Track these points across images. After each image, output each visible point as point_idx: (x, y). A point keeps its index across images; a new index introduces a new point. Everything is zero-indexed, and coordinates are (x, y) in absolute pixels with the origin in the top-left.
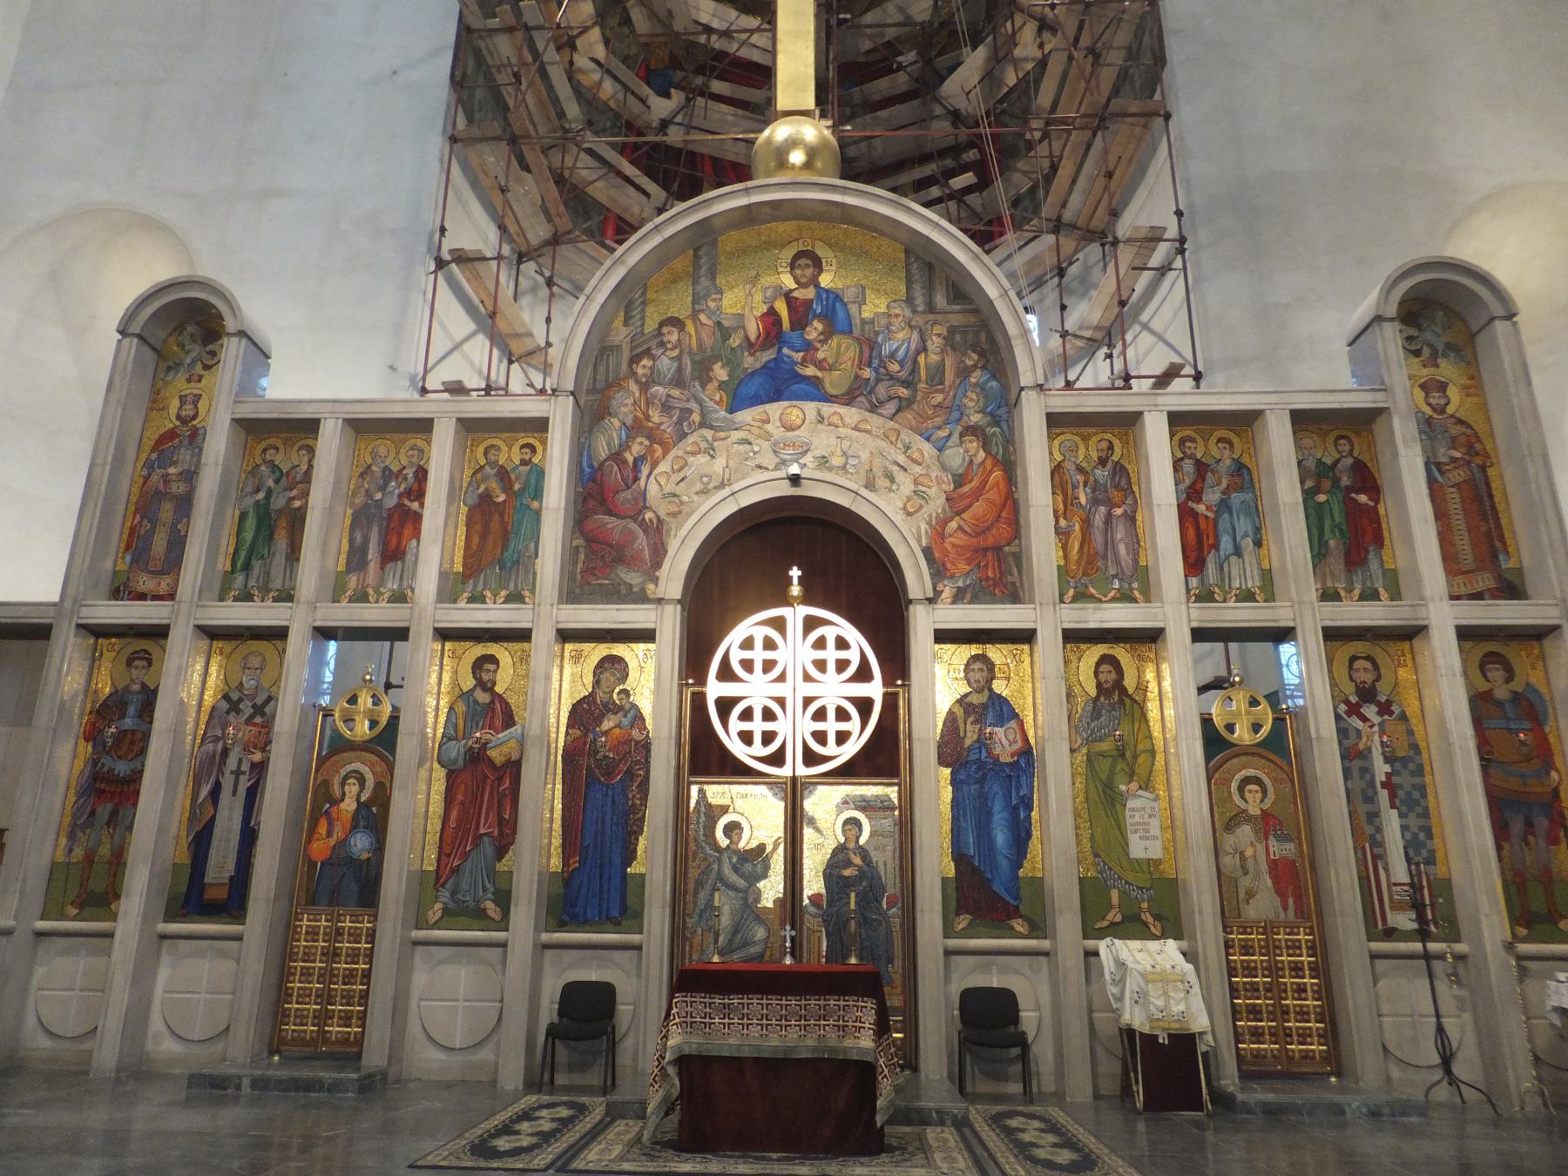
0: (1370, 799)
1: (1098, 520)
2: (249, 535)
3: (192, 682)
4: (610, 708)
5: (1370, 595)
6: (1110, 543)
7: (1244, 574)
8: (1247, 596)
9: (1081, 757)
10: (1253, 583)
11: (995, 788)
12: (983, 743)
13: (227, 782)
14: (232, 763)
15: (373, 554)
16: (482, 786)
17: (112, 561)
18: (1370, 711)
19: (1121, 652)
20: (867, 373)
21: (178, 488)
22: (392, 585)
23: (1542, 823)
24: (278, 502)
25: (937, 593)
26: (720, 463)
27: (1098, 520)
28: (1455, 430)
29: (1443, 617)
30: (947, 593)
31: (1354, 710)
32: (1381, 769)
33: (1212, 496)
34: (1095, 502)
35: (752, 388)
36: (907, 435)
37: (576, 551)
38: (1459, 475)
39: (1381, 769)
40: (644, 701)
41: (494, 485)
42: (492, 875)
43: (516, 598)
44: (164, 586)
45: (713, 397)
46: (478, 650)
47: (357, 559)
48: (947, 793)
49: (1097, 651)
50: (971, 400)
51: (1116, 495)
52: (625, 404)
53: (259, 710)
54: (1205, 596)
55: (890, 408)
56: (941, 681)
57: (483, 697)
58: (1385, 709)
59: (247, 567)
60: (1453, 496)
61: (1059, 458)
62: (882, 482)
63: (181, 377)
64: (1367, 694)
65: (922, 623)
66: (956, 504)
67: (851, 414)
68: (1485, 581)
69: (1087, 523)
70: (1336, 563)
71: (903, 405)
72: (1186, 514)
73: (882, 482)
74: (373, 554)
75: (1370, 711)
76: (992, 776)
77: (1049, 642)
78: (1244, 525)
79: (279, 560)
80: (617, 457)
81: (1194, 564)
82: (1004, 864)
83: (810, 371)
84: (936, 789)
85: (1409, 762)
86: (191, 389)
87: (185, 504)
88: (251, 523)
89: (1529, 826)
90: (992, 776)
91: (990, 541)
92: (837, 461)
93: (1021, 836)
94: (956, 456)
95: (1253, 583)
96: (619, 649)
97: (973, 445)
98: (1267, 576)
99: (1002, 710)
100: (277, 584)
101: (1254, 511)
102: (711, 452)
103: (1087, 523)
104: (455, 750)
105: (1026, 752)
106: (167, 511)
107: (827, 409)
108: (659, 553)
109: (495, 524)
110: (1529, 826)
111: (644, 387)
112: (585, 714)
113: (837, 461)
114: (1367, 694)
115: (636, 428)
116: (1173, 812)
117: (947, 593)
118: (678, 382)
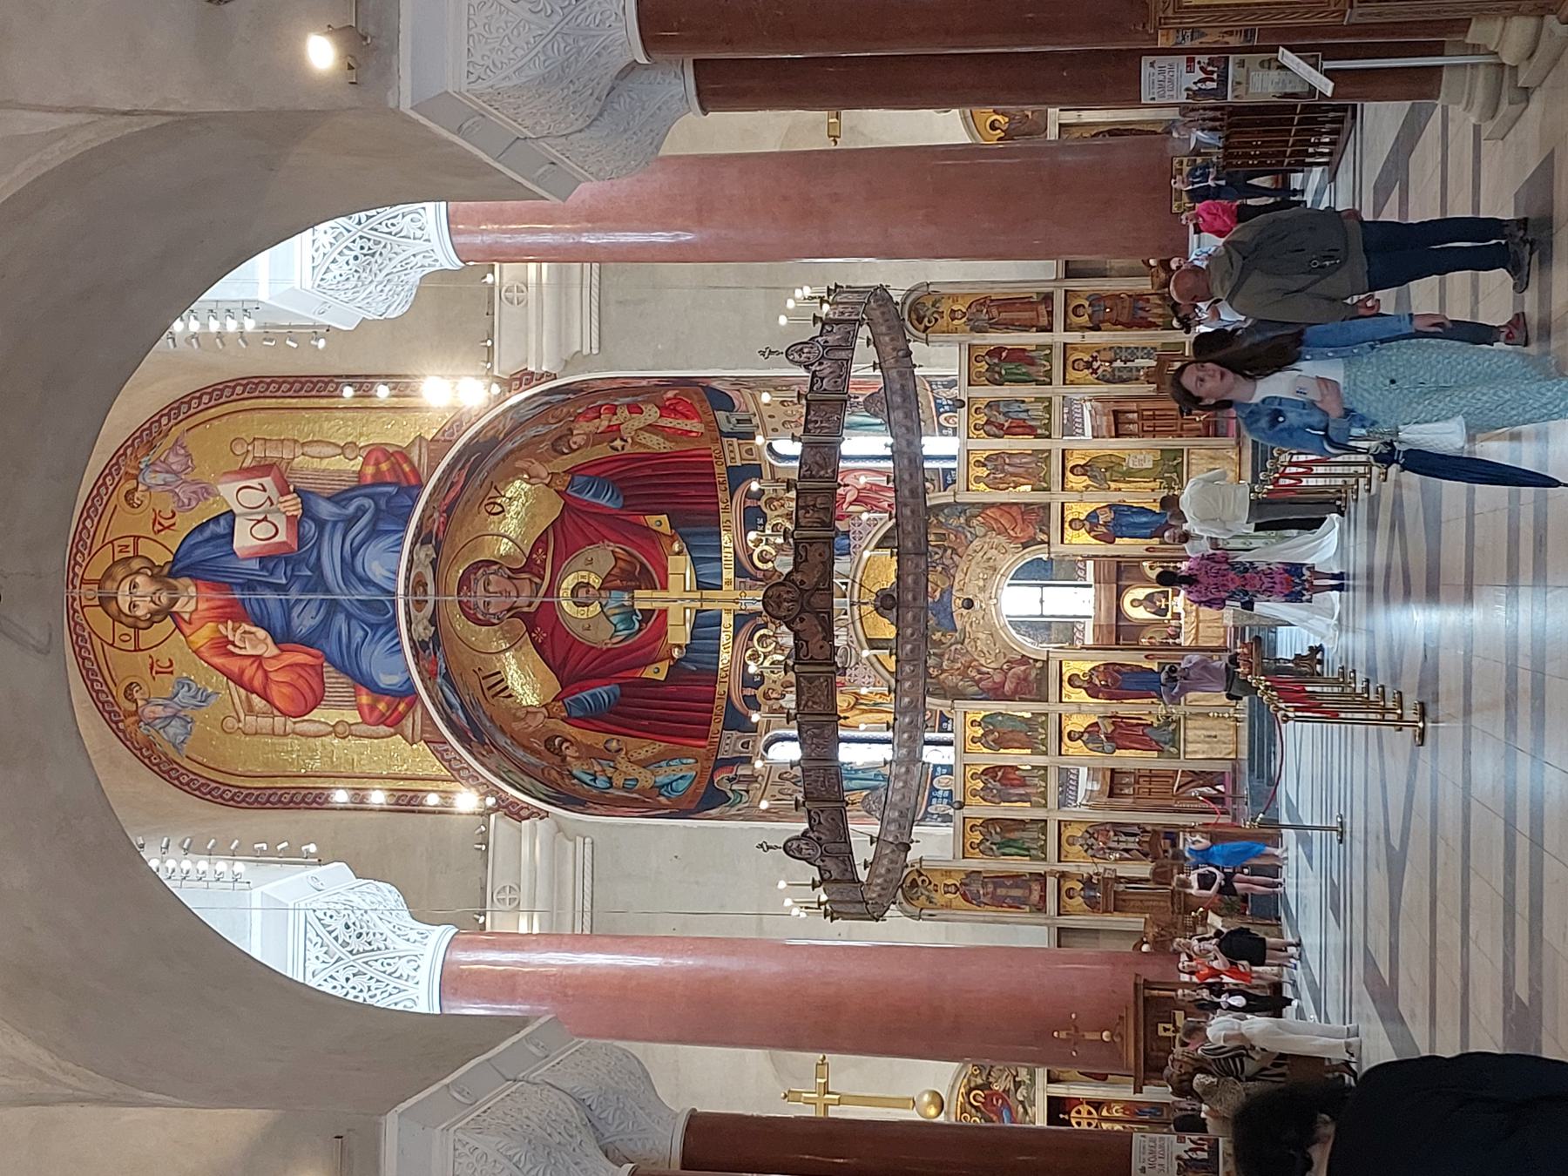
0: (1131, 369)
1: (1011, 469)
2: (1013, 850)
3: (1082, 865)
4: (1090, 681)
5: (1048, 358)
6: (1021, 465)
7: (1037, 410)
8: (1048, 409)
9: (1113, 485)
10: (1041, 406)
11: (1125, 520)
12: (1106, 524)
13: (1123, 846)
14: (1114, 845)
15: (1022, 791)
16: (1122, 733)
17: (1024, 915)
18: (1096, 365)
19: (1069, 465)
20: (939, 568)
21: (990, 888)
22: (1036, 781)
23: (1141, 304)
24: (998, 839)
25: (1043, 542)
26: (980, 635)
27: (1011, 469)
28: (974, 309)
29: (1059, 336)
30: (1044, 537)
31: (1095, 371)
32: (1118, 364)
33: (1001, 419)
34: (1003, 471)
35: (946, 622)
36: (970, 551)
37: (1021, 700)
38: (995, 312)
39: (1118, 364)
40: (1088, 666)
41: (990, 738)
42: (1159, 727)
43: (1044, 725)
44: (1036, 887)
45: (948, 640)
46: (1065, 739)
47: (1023, 798)
48: (1126, 540)
49: (1068, 474)
50: (954, 522)
51: (1000, 461)
52: (951, 680)
53: (1092, 835)
54: (1048, 426)
55: (956, 558)
56: (1081, 540)
57: (1086, 736)
58: (1095, 359)
59: (1028, 849)
60: (1003, 315)
61: (982, 486)
62: (991, 563)
63: (933, 895)
64: (1089, 365)
65: (1057, 548)
66: (1003, 531)
67: (959, 576)
68: (1042, 309)
69: (1012, 475)
70: (1032, 369)
71: (954, 551)
72: (1010, 432)
73: (991, 563)
74: (1022, 791)
75: (1096, 365)
76: (1121, 521)
77: (1063, 497)
78: (1015, 407)
79: (1025, 834)
80: (977, 683)
81: (1031, 431)
82: (1155, 518)
83: (938, 594)
84: (1127, 546)
85: (1117, 352)
86: (941, 889)
87: (999, 879)
88: (1007, 850)
89: (1142, 309)
90: (1121, 521)
91: (1019, 517)
92: (981, 583)
93: (1143, 511)
94: (980, 531)
95: (1041, 406)
96: (1065, 678)
97: (974, 522)
98: (1037, 400)
99: (1093, 516)
100: (1035, 835)
101: (1008, 402)
102: (975, 640)
103: (1012, 475)
104: (1108, 747)
105: (1110, 506)
106: (1001, 892)
107: (956, 587)
108: (1024, 660)
109: (1010, 736)
110: (1142, 309)
111: (943, 671)
112: (1093, 692)
113: (981, 583)
114: (1089, 365)
115: (964, 675)
116: (1138, 451)
117: (1044, 537)
118: (941, 656)
